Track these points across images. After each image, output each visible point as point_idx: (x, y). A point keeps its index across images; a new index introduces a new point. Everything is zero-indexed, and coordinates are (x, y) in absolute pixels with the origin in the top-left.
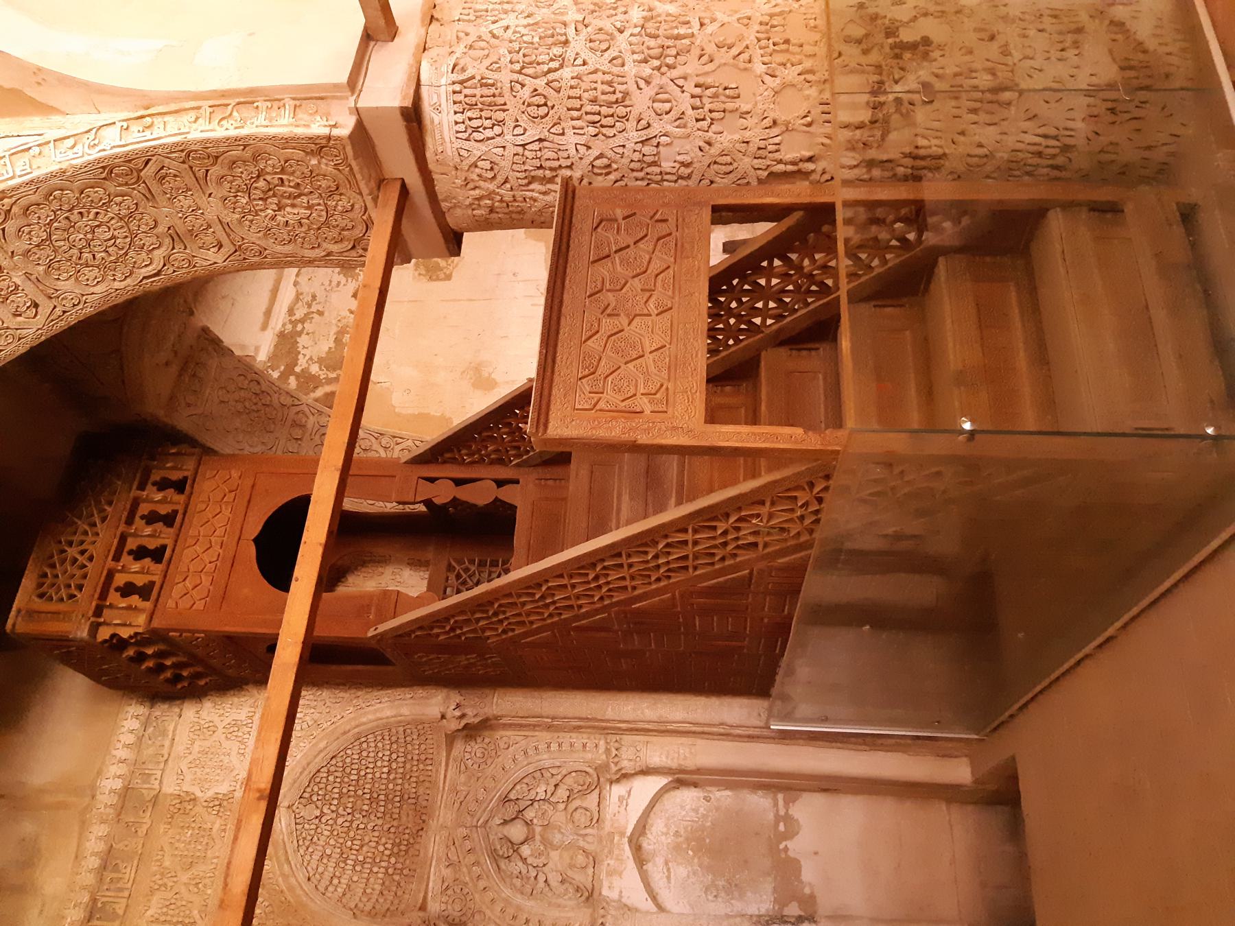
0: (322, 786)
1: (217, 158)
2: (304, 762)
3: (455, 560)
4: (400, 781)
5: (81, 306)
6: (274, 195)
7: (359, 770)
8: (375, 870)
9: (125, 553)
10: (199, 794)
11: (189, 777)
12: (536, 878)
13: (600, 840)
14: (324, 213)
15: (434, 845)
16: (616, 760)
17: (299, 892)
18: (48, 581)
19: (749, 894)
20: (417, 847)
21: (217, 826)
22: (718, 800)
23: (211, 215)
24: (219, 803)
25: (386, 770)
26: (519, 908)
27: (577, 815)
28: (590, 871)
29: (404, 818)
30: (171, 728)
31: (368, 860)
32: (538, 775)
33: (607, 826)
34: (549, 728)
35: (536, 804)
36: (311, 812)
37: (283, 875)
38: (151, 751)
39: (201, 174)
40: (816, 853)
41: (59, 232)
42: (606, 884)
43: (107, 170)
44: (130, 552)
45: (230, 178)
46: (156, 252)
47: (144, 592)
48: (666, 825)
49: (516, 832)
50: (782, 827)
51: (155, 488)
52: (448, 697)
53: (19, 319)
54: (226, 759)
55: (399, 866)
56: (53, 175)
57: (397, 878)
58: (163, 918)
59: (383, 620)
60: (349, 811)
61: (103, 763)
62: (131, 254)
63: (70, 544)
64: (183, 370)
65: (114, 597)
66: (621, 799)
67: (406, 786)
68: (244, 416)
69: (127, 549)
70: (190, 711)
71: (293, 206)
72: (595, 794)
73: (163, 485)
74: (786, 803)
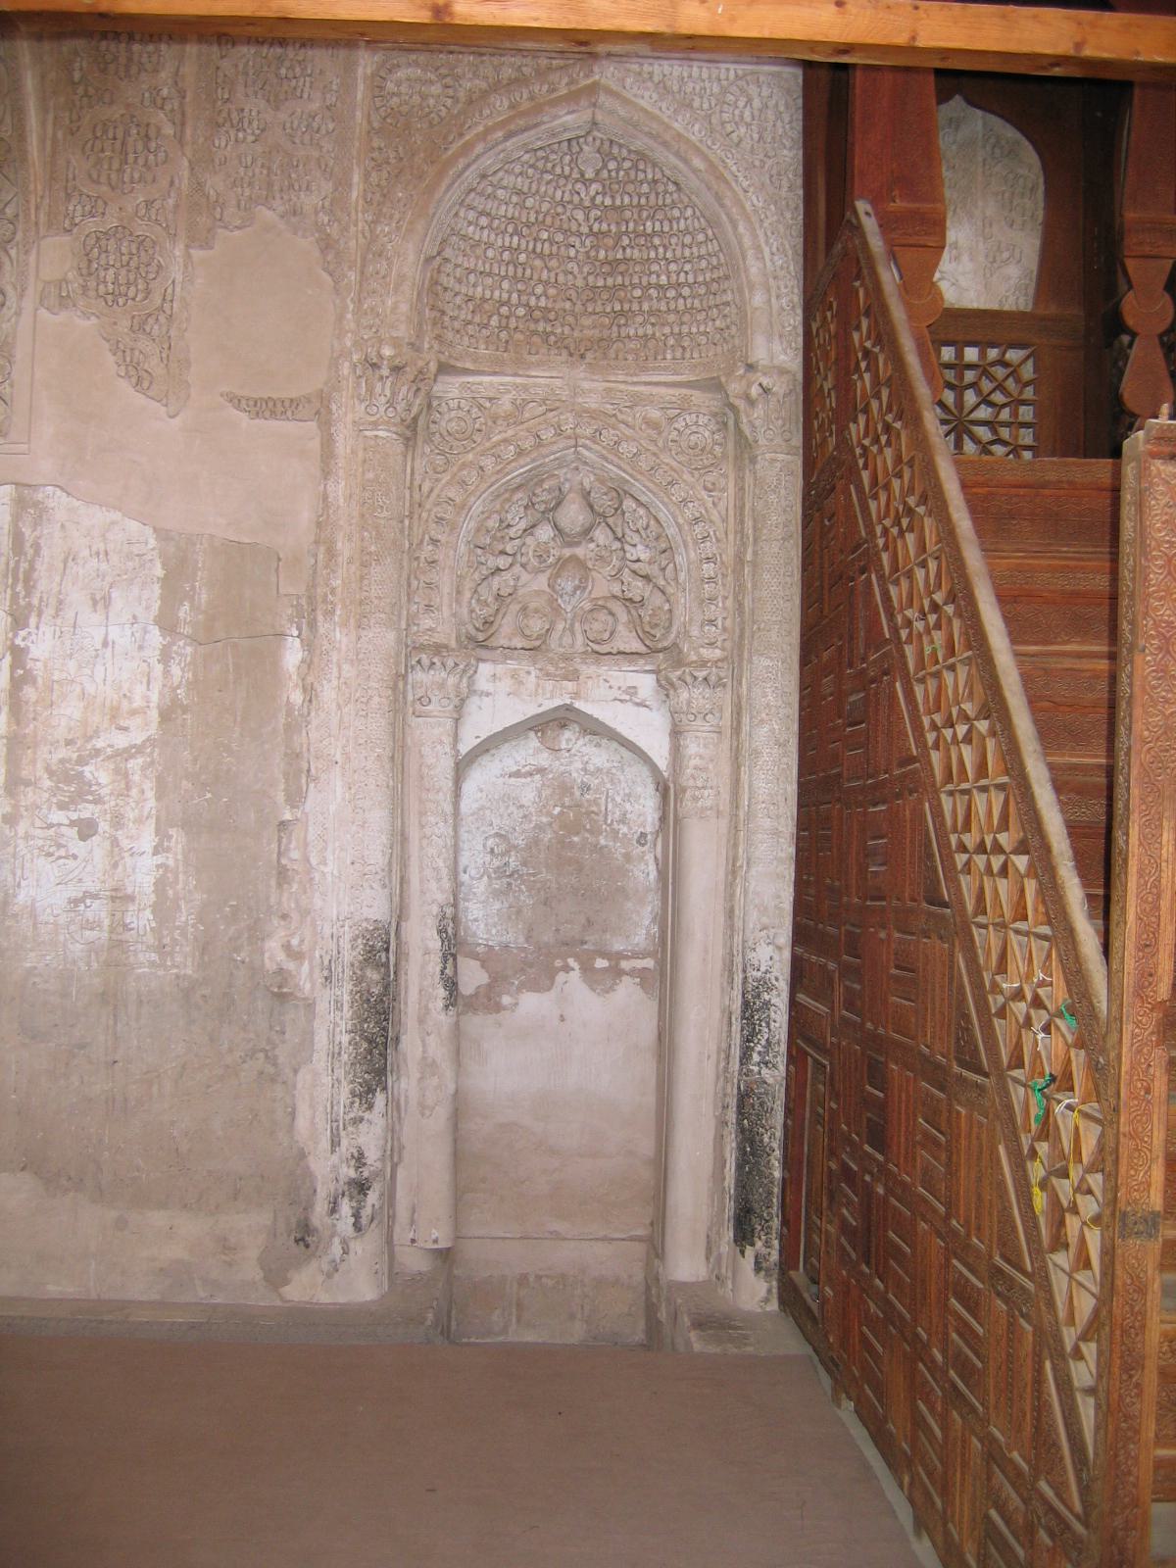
0: (632, 173)
2: (668, 137)
4: (646, 307)
8: (506, 285)
12: (503, 553)
13: (567, 658)
15: (548, 378)
16: (689, 679)
19: (497, 905)
20: (544, 350)
22: (641, 858)
26: (454, 528)
27: (603, 616)
28: (518, 642)
29: (587, 321)
31: (520, 271)
32: (664, 546)
33: (588, 670)
34: (739, 559)
35: (617, 545)
37: (488, 131)
40: (562, 1018)
42: (500, 669)
48: (599, 770)
49: (573, 515)
50: (601, 963)
52: (782, 371)
60: (596, 228)
66: (632, 691)
67: (640, 319)
72: (636, 646)
74: (642, 975)
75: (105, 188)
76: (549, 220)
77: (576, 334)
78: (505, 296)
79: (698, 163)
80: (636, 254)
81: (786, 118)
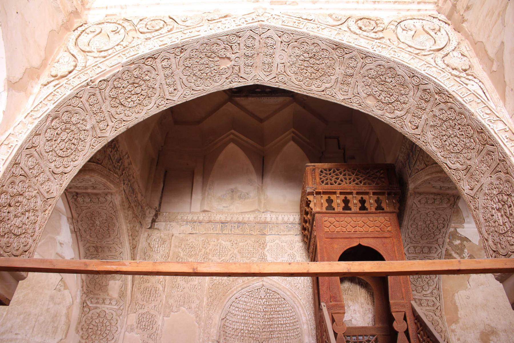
1: (508, 173)
2: (281, 288)
3: (376, 339)
4: (278, 329)
5: (424, 144)
6: (503, 205)
7: (281, 311)
8: (242, 325)
9: (344, 196)
10: (266, 249)
11: (272, 244)
14: (504, 232)
17: (231, 296)
18: (328, 172)
21: (255, 259)
23: (483, 180)
24: (263, 258)
25: (282, 322)
29: (263, 334)
30: (292, 233)
36: (262, 294)
37: (237, 288)
38: (282, 228)
39: (498, 169)
41: (449, 124)
43: (481, 130)
44: (346, 198)
45: (502, 183)
46: (458, 164)
47: (330, 207)
51: (376, 199)
53: (409, 124)
54: (280, 257)
55: (244, 335)
56: (469, 111)
57: (240, 334)
58: (221, 247)
59: (328, 309)
60: (265, 310)
61: (276, 212)
62: (453, 155)
63: (345, 175)
64: (435, 194)
65: (325, 197)
67: (277, 333)
68: (424, 225)
69: (347, 196)
70: (298, 238)
71: (502, 216)
73: (378, 201)
75: (145, 302)
76: (253, 309)
77: (261, 337)
78: (242, 328)
79: (288, 293)
80: (275, 316)
81: (310, 281)
